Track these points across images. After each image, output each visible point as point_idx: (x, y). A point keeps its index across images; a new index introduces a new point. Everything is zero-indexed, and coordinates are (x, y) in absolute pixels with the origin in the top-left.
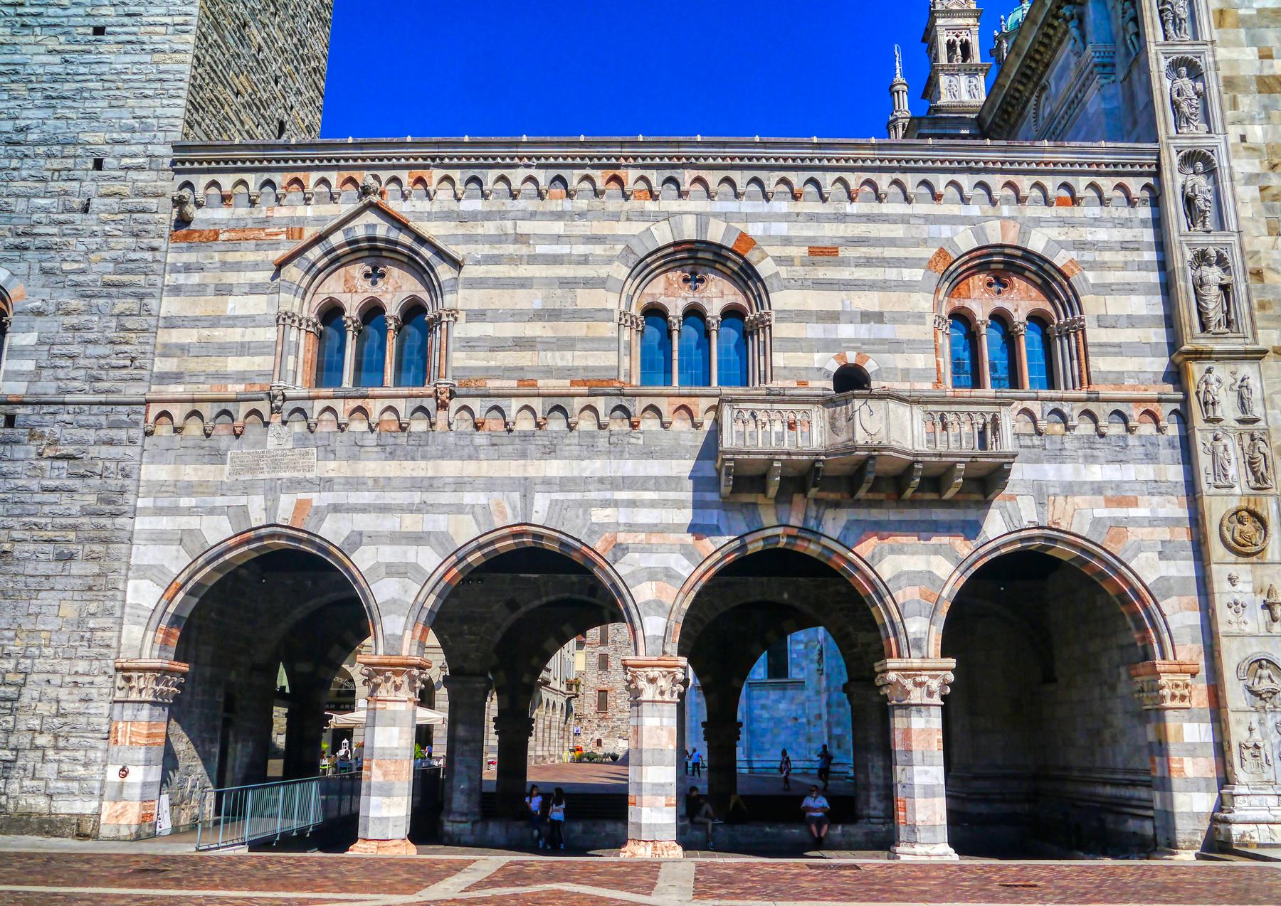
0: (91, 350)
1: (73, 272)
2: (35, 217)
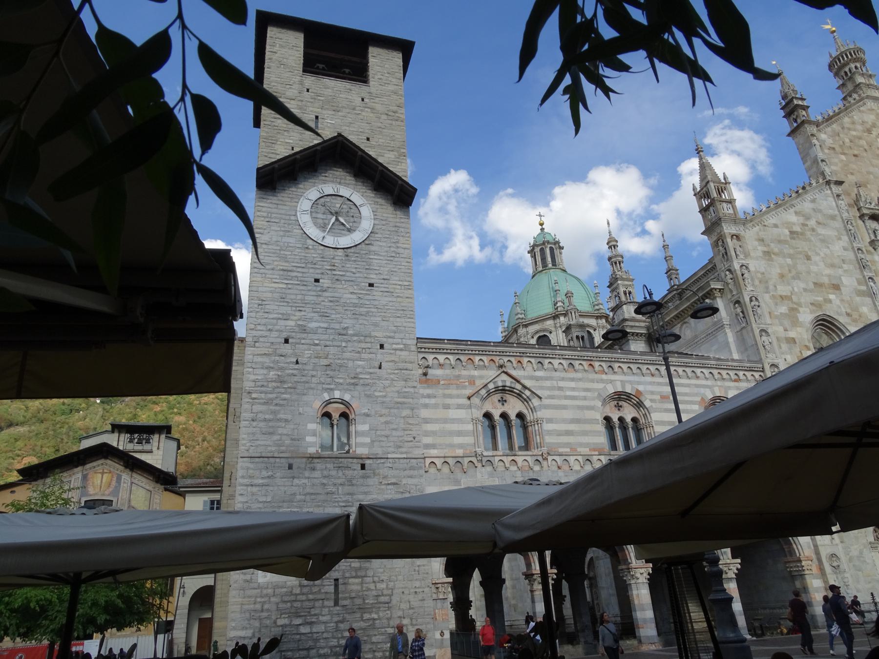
0: (394, 433)
1: (380, 396)
2: (358, 370)
